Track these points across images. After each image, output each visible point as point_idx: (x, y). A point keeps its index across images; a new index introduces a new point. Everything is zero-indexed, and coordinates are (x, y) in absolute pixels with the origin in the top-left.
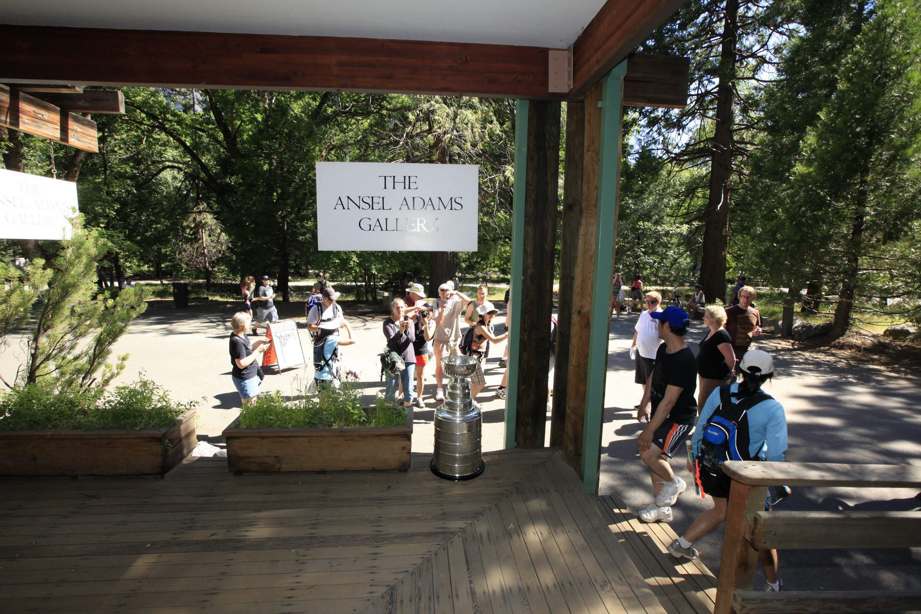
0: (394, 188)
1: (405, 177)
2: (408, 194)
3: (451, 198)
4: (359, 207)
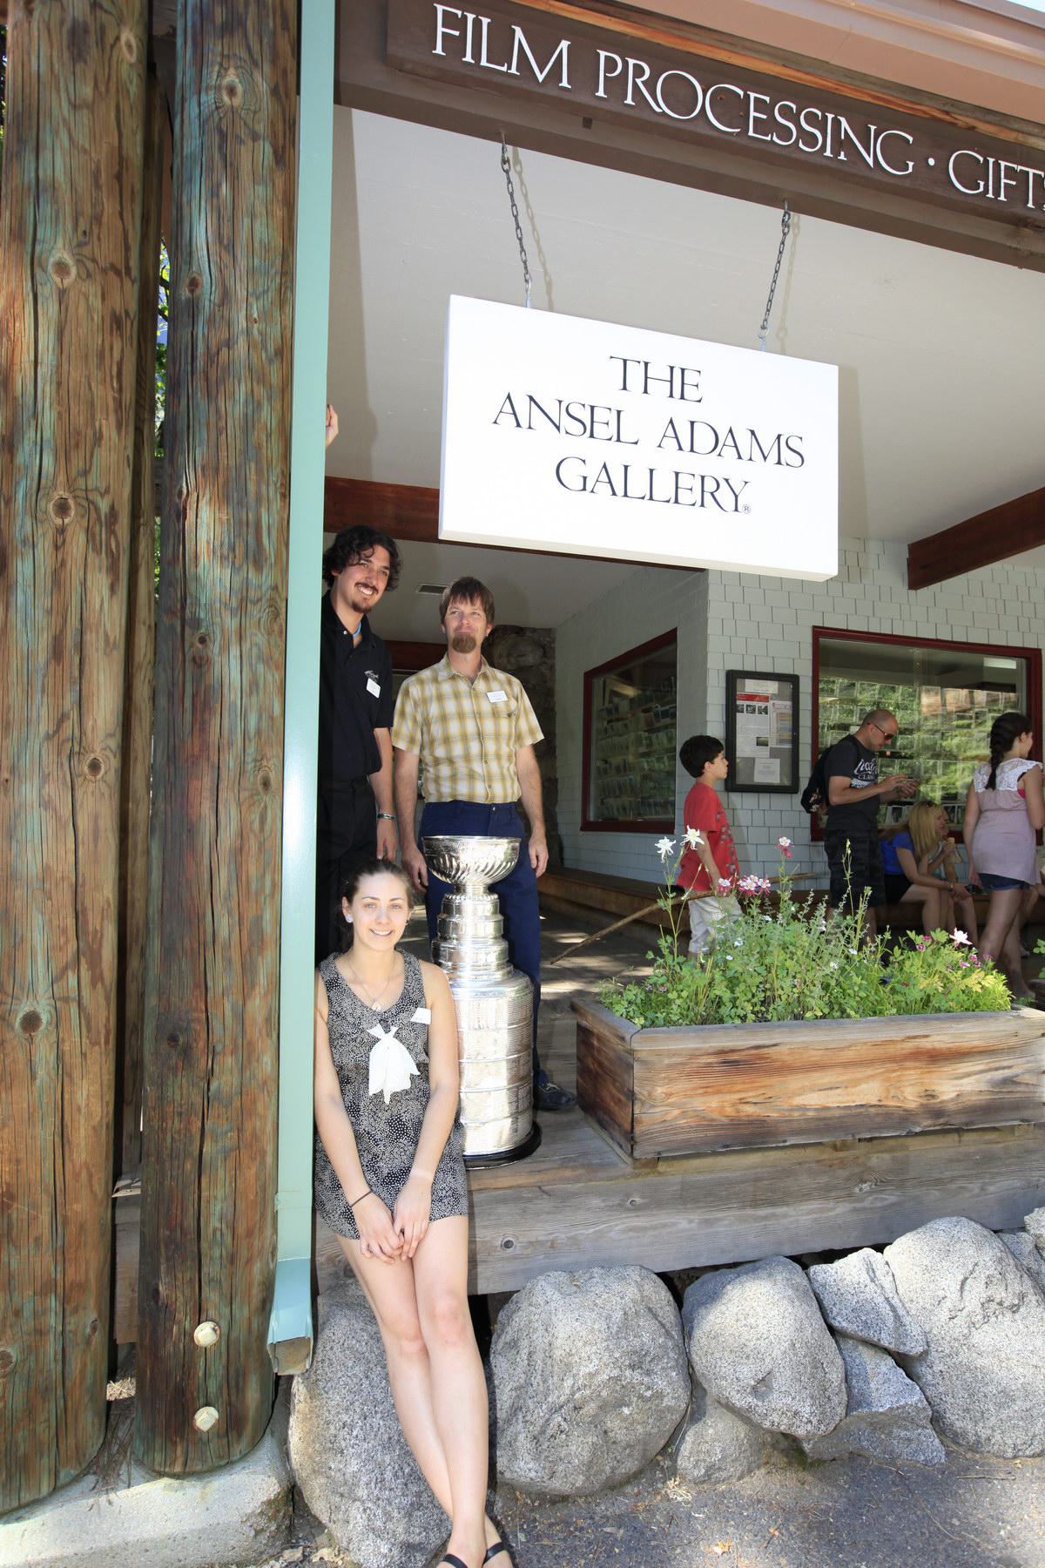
0: (646, 392)
1: (672, 368)
2: (682, 413)
3: (779, 437)
4: (558, 428)
